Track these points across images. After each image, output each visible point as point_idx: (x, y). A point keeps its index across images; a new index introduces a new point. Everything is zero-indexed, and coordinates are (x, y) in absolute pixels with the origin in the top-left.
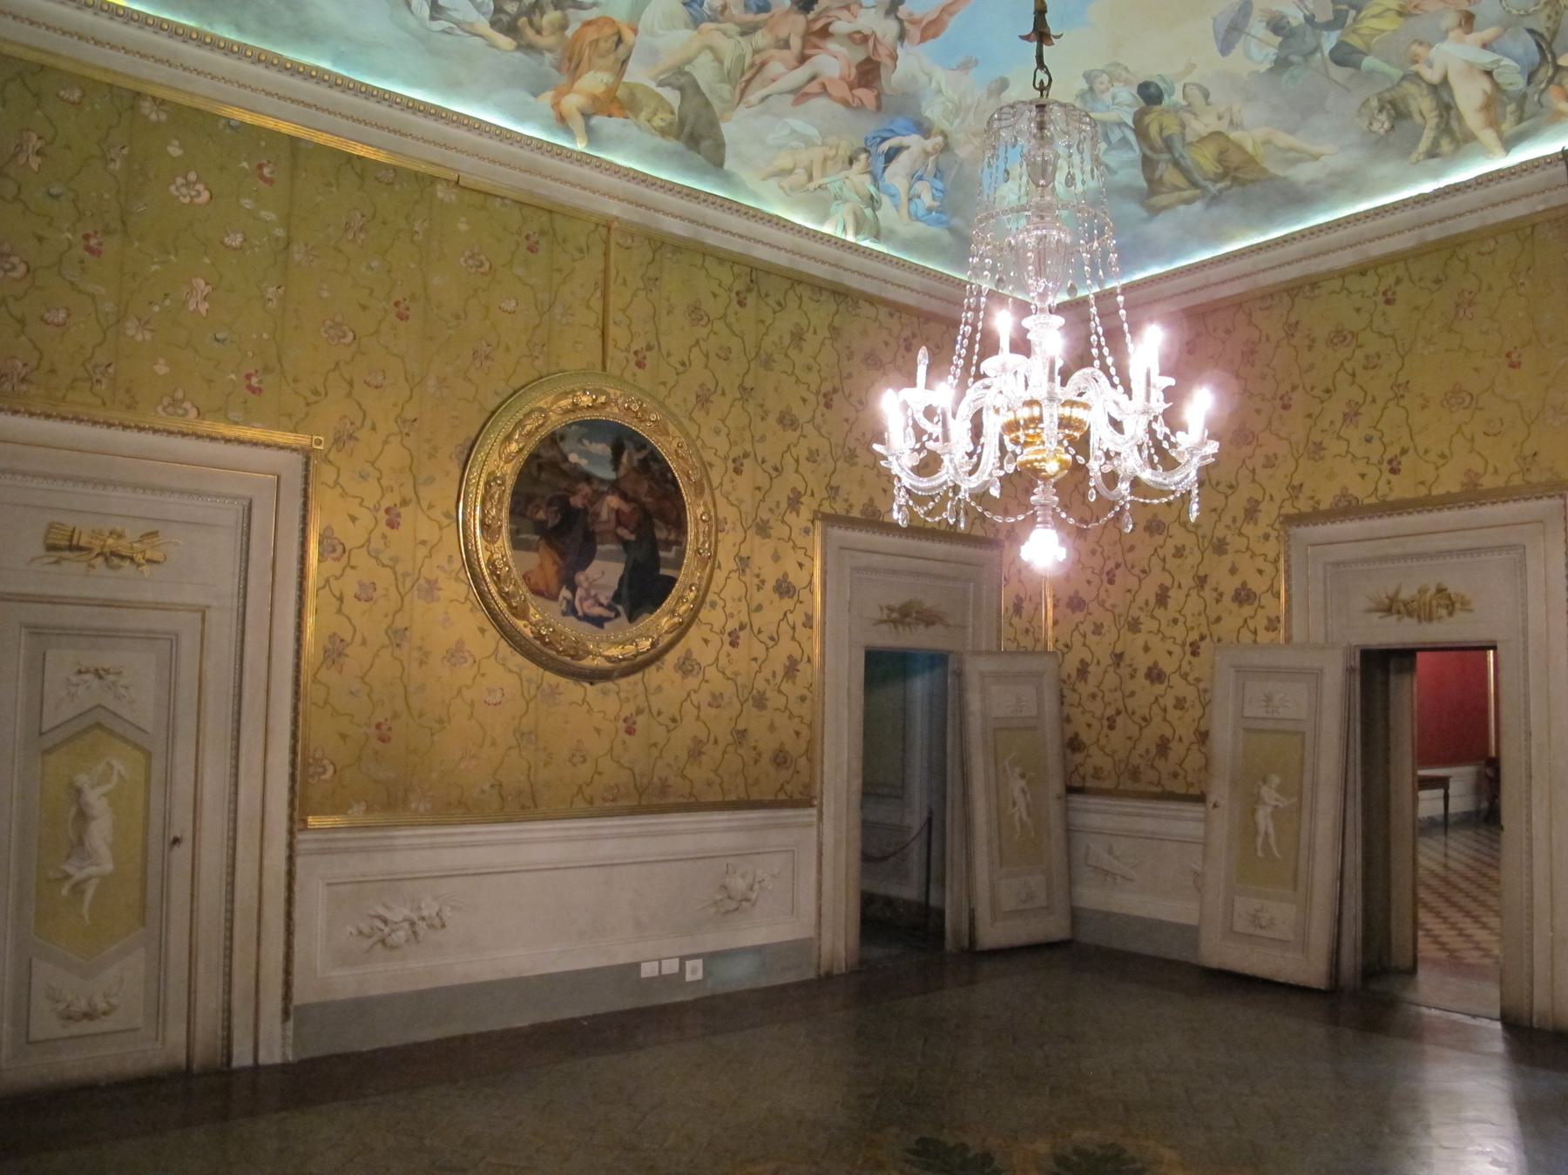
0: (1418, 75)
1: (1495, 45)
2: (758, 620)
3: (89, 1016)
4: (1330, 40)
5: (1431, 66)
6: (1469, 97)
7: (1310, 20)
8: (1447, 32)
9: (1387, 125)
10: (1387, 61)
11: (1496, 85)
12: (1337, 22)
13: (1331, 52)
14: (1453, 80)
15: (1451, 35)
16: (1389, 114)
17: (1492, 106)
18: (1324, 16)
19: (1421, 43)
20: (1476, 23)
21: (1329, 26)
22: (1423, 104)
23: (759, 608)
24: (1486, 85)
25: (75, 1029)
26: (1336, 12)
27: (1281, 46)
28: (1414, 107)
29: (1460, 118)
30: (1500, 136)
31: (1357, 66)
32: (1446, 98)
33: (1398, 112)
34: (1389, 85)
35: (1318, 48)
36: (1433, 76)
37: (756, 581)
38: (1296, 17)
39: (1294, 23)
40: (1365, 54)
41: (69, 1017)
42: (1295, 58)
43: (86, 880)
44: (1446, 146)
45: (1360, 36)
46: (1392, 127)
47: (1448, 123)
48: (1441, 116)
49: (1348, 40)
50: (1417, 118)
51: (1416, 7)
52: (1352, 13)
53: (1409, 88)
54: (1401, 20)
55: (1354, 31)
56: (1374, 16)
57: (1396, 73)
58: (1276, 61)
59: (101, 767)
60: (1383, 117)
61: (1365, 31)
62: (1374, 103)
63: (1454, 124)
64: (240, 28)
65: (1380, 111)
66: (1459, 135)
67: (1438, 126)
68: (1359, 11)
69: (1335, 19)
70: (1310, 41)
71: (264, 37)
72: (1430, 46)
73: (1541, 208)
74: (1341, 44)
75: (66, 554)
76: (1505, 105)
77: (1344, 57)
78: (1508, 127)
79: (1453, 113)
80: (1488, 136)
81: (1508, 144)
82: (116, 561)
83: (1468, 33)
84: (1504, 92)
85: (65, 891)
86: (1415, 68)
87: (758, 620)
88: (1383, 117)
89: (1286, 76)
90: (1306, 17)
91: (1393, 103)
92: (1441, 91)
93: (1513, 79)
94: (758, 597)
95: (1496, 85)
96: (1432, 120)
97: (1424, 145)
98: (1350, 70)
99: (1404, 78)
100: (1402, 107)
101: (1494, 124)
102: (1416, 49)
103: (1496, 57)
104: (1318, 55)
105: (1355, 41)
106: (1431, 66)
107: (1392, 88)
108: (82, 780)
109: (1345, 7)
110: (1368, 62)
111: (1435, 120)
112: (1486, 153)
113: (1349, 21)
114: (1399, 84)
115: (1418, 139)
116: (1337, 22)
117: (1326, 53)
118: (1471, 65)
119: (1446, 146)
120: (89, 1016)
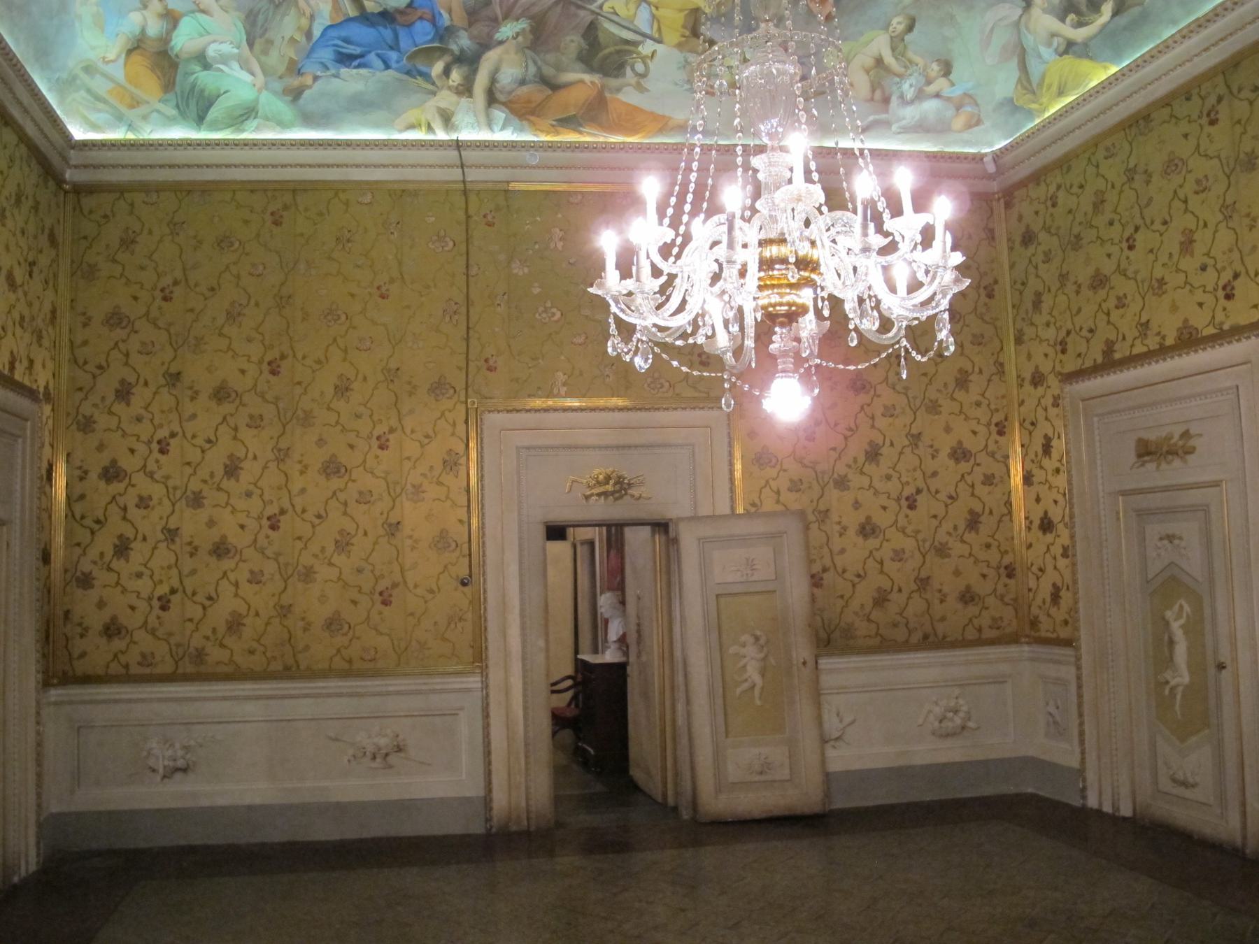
2: (934, 484)
3: (1185, 784)
23: (935, 474)
25: (1181, 791)
37: (930, 450)
41: (1174, 780)
43: (1178, 685)
59: (1176, 607)
64: (1174, 22)
71: (1189, 13)
75: (1146, 458)
82: (1170, 457)
85: (1167, 692)
87: (934, 484)
94: (930, 465)
108: (1169, 614)
120: (1185, 784)
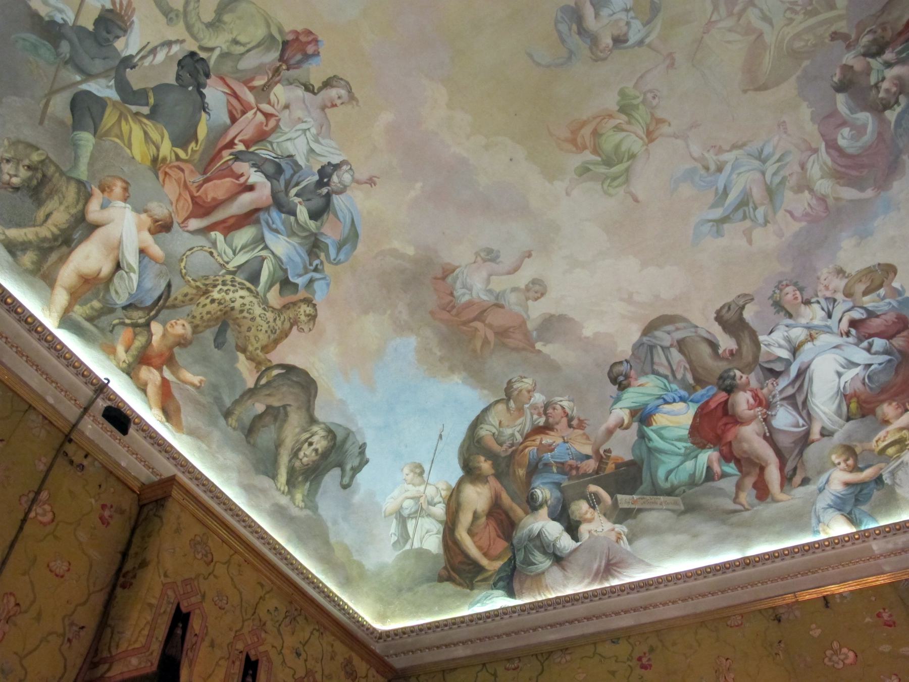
0: (88, 197)
1: (147, 259)
4: (102, 88)
5: (103, 207)
6: (89, 257)
7: (127, 62)
8: (146, 211)
9: (15, 180)
10: (93, 160)
11: (110, 279)
12: (128, 95)
13: (88, 93)
14: (99, 234)
15: (144, 216)
16: (30, 179)
17: (90, 286)
18: (136, 79)
19: (126, 189)
20: (163, 236)
21: (123, 87)
22: (59, 215)
24: (106, 269)
26: (144, 92)
27: (80, 30)
28: (50, 205)
29: (63, 259)
30: (67, 310)
31: (77, 125)
32: (77, 236)
33: (38, 189)
34: (64, 169)
35: (89, 76)
36: (94, 211)
38: (129, 45)
39: (119, 44)
40: (95, 134)
42: (65, 47)
44: (28, 258)
45: (119, 121)
46: (16, 189)
47: (51, 249)
48: (55, 238)
49: (108, 111)
50: (41, 214)
51: (166, 174)
52: (146, 110)
53: (71, 192)
54: (148, 163)
55: (121, 116)
56: (146, 133)
57: (82, 172)
58: (53, 23)
60: (24, 173)
61: (124, 127)
62: (35, 157)
63: (54, 257)
65: (29, 168)
66: (45, 267)
67: (45, 239)
68: (147, 117)
69: (134, 92)
70: (98, 65)
72: (125, 200)
73: (51, 400)
74: (101, 103)
76: (96, 296)
77: (85, 110)
78: (79, 312)
79: (64, 249)
80: (61, 297)
81: (66, 322)
83: (149, 230)
84: (107, 290)
86: (97, 191)
88: (24, 173)
89: (33, 38)
90: (131, 57)
91: (44, 180)
92: (81, 227)
93: (124, 289)
95: (110, 279)
96: (45, 232)
97: (14, 233)
98: (67, 117)
99: (80, 182)
100: (46, 190)
101: (75, 296)
102: (118, 189)
103: (135, 265)
104: (78, 78)
105: (109, 118)
106: (103, 207)
107: (62, 174)
109: (152, 101)
110: (87, 139)
111: (49, 235)
112: (48, 303)
113: (134, 108)
114: (69, 179)
115: (19, 225)
116: (128, 95)
117: (84, 87)
118: (120, 244)
119: (28, 258)
